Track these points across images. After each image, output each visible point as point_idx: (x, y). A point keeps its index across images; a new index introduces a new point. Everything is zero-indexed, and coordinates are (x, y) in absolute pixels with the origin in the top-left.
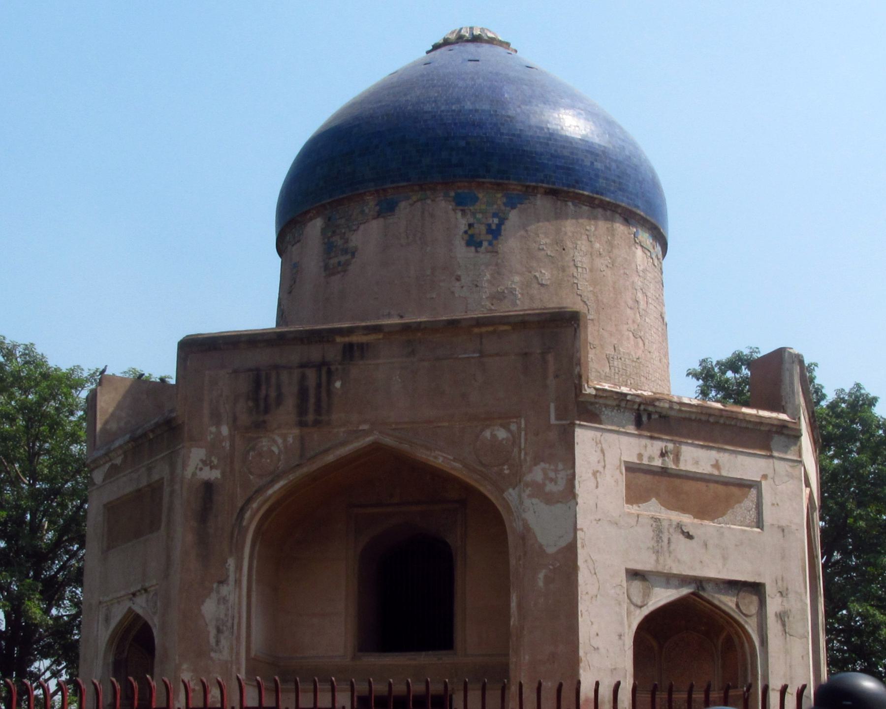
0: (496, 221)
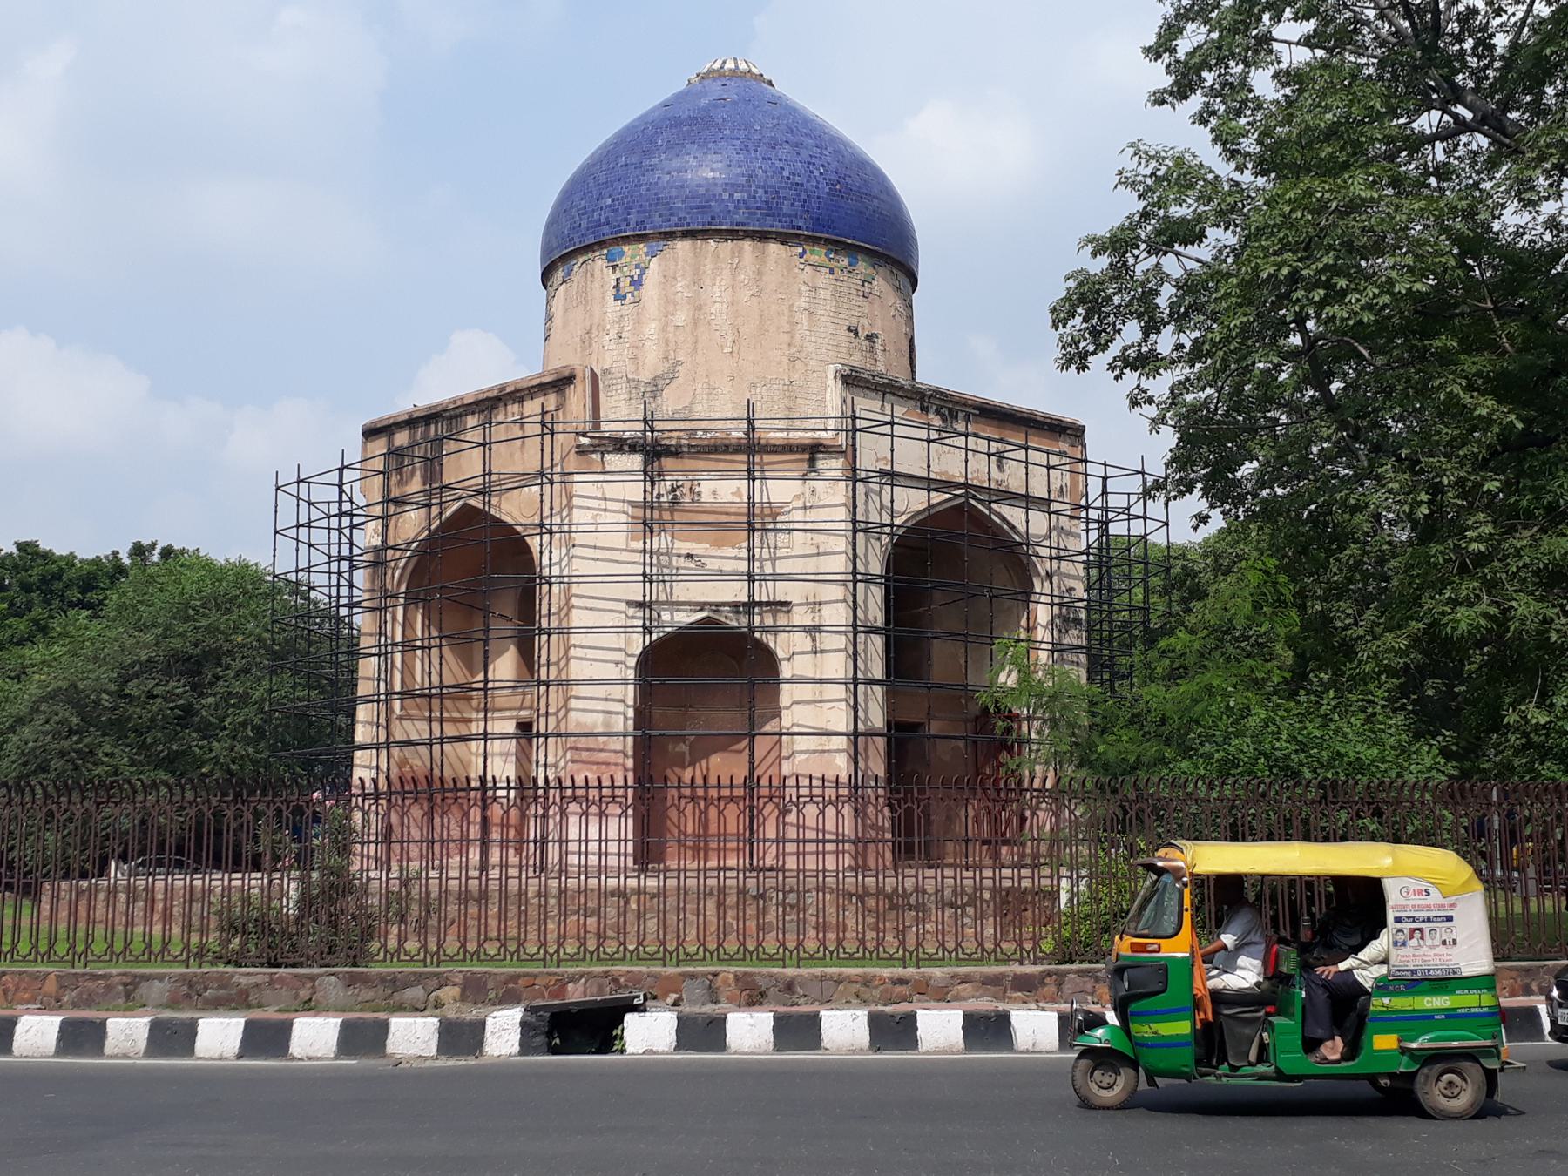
0: (638, 271)
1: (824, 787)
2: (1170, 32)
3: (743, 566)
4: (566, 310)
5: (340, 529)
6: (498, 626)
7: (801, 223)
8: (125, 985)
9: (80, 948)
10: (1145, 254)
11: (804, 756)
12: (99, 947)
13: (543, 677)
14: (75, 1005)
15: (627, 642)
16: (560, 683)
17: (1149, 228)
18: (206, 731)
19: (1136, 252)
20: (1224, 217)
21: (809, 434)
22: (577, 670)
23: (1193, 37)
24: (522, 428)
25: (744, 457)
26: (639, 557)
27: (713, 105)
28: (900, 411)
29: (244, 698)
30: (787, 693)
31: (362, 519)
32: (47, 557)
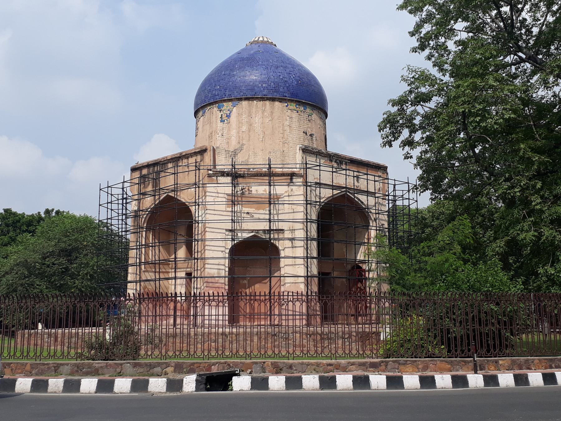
0: (229, 112)
2: (418, 27)
3: (267, 217)
4: (203, 126)
6: (179, 238)
10: (410, 106)
11: (289, 285)
15: (226, 244)
16: (202, 259)
19: (407, 105)
21: (290, 170)
22: (208, 254)
23: (427, 28)
24: (188, 168)
25: (267, 178)
26: (230, 214)
27: (256, 53)
28: (322, 161)
30: (283, 262)
31: (131, 200)
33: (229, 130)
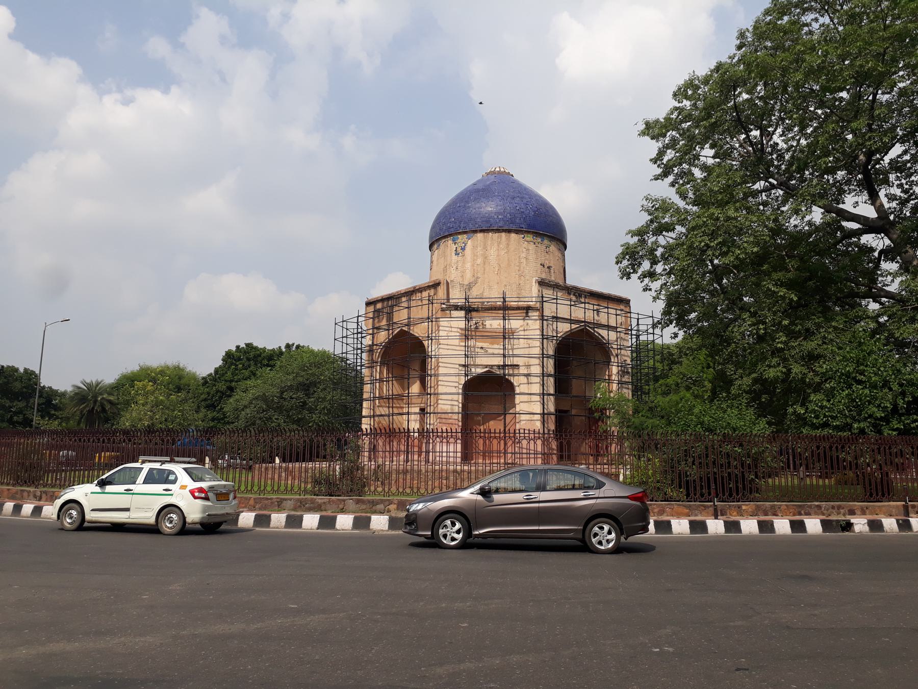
1: (529, 433)
2: (661, 153)
5: (357, 339)
6: (412, 373)
7: (523, 226)
8: (278, 502)
9: (262, 489)
10: (652, 236)
11: (524, 422)
12: (269, 488)
13: (429, 392)
14: (260, 509)
15: (459, 379)
17: (653, 227)
18: (311, 411)
19: (648, 235)
20: (681, 222)
21: (526, 303)
22: (441, 389)
23: (670, 155)
24: (422, 302)
25: (502, 312)
26: (463, 348)
27: (491, 184)
28: (559, 294)
29: (324, 399)
30: (518, 399)
31: (365, 335)
32: (256, 348)
33: (464, 263)
